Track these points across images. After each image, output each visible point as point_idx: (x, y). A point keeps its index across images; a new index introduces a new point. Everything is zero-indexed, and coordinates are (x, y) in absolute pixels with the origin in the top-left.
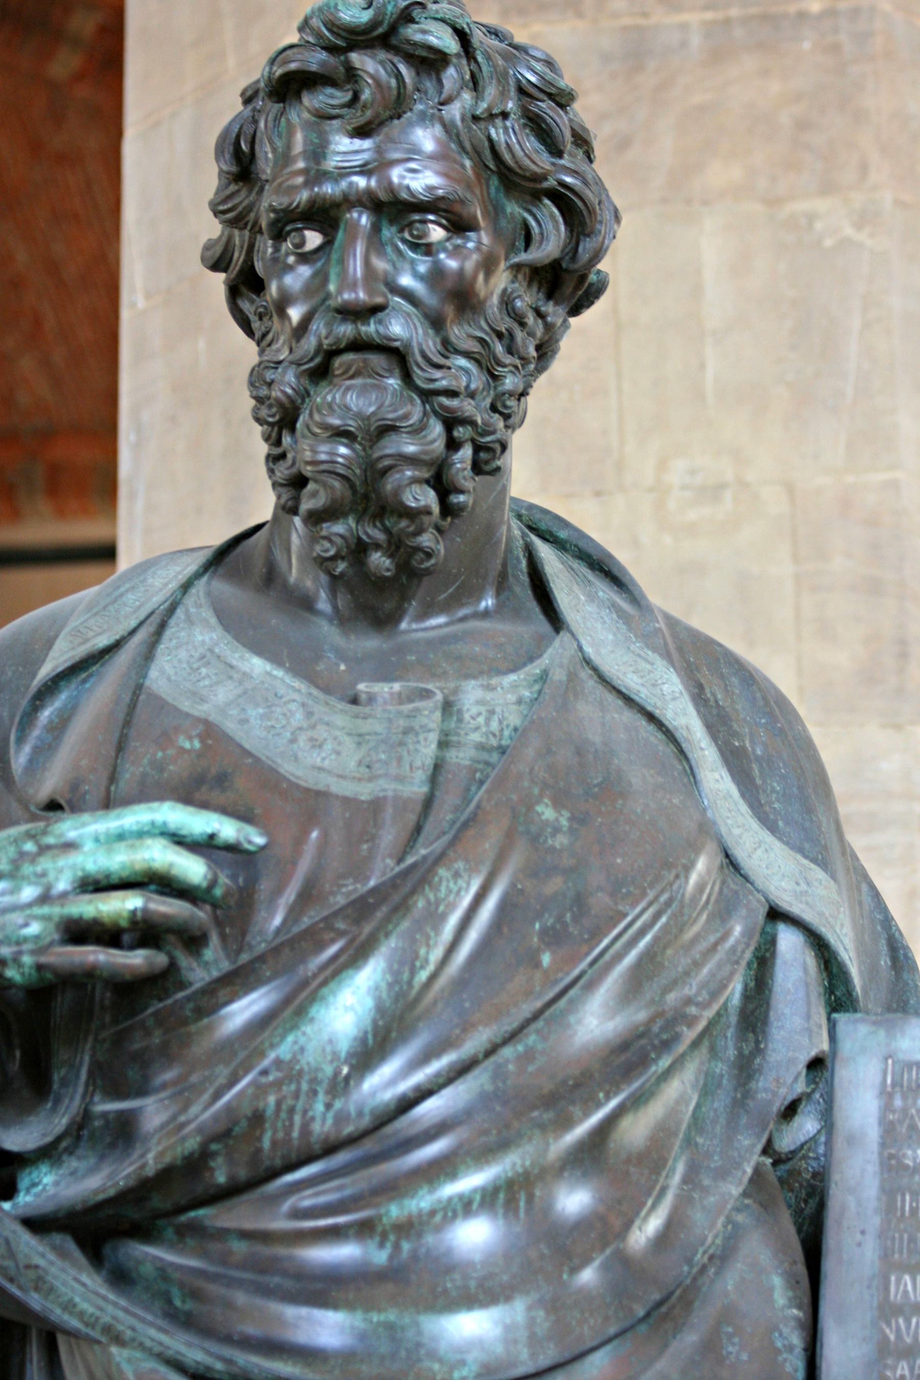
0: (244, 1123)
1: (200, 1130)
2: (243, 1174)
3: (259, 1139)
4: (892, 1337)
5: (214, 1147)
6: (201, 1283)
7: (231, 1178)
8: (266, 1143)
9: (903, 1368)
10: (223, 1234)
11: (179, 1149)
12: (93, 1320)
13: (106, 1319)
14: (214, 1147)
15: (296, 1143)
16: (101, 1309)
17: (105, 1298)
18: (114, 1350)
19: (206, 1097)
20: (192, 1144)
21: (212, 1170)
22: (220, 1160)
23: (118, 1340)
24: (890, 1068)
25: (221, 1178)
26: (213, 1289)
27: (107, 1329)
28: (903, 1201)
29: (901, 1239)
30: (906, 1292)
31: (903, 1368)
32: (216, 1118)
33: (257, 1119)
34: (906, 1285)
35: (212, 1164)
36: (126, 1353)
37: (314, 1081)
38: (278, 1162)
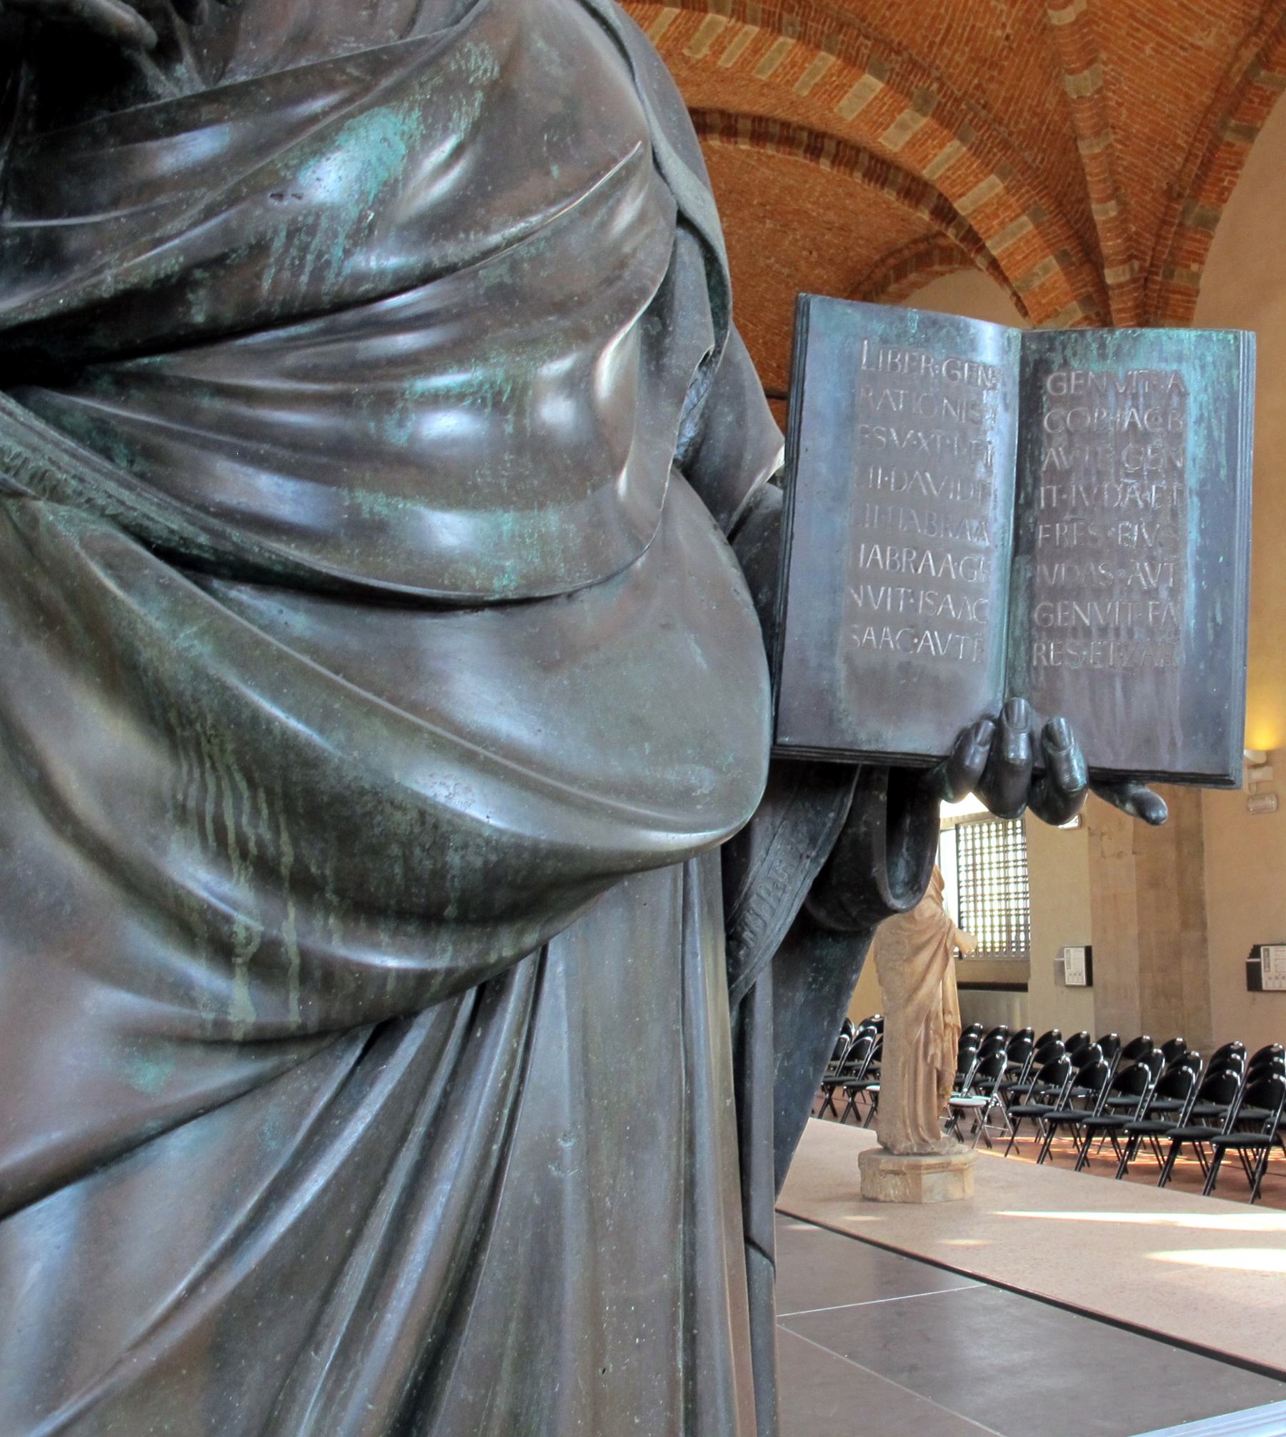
0: (243, 252)
1: (183, 249)
2: (228, 314)
3: (259, 276)
4: (860, 603)
5: (198, 274)
6: (160, 440)
7: (212, 319)
8: (266, 285)
9: (869, 634)
10: (192, 386)
11: (153, 269)
12: (18, 462)
13: (43, 464)
14: (198, 274)
15: (303, 288)
16: (35, 450)
17: (41, 435)
18: (41, 506)
19: (194, 212)
20: (172, 265)
21: (189, 305)
22: (202, 293)
23: (56, 494)
24: (866, 348)
25: (199, 318)
26: (178, 449)
27: (38, 478)
28: (876, 475)
29: (873, 511)
30: (875, 562)
31: (869, 634)
32: (209, 238)
33: (260, 248)
34: (875, 554)
35: (191, 297)
36: (63, 510)
37: (334, 218)
38: (276, 309)
